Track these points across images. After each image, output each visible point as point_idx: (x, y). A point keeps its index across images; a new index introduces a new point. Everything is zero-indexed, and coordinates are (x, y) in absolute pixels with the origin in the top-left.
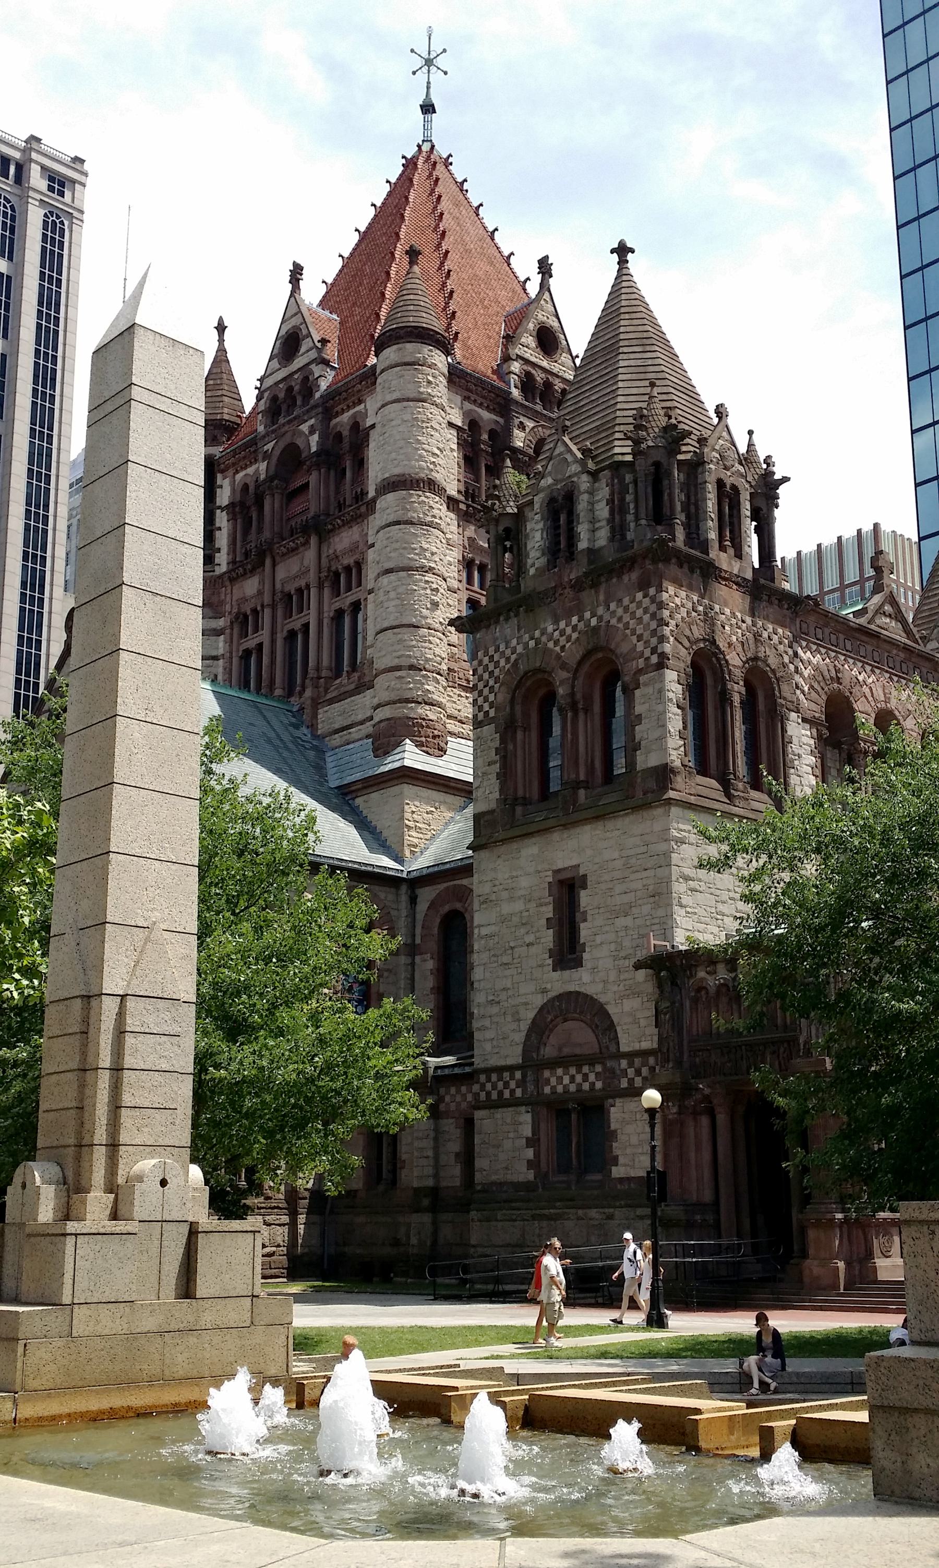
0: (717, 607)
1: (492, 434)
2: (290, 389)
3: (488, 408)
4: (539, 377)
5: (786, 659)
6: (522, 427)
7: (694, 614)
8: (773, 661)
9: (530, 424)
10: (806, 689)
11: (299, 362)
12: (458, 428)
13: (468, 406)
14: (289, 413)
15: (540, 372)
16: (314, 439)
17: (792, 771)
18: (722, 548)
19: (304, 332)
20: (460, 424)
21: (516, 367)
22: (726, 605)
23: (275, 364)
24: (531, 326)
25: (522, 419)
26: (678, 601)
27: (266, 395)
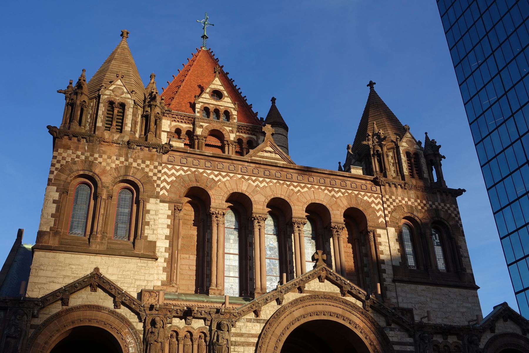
0: (96, 155)
4: (212, 108)
5: (151, 174)
6: (201, 126)
7: (76, 159)
8: (139, 176)
9: (205, 125)
10: (168, 187)
12: (168, 132)
13: (174, 124)
17: (146, 227)
18: (108, 129)
20: (169, 130)
22: (104, 153)
24: (208, 90)
25: (201, 124)
26: (65, 155)
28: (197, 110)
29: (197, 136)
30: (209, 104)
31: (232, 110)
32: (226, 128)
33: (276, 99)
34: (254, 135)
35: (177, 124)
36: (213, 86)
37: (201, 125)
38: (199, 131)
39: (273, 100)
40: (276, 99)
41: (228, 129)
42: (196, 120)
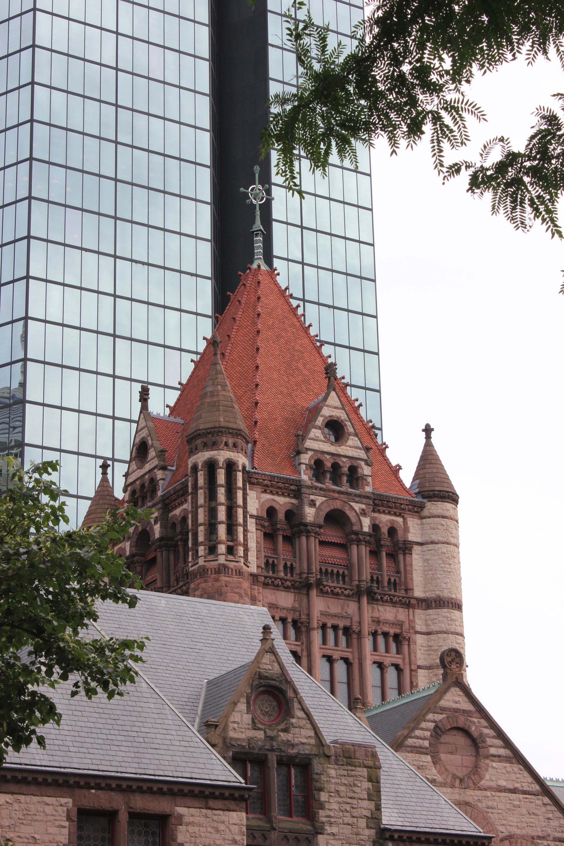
1: (289, 514)
2: (143, 486)
3: (283, 495)
6: (312, 504)
9: (319, 500)
11: (147, 467)
14: (152, 498)
15: (328, 457)
16: (157, 528)
19: (150, 442)
21: (305, 458)
23: (134, 466)
24: (320, 421)
25: (312, 497)
27: (129, 488)
28: (303, 467)
29: (306, 525)
30: (323, 452)
31: (362, 463)
32: (352, 504)
33: (433, 430)
34: (400, 515)
35: (269, 496)
36: (326, 412)
37: (312, 501)
38: (310, 514)
39: (428, 430)
40: (433, 430)
41: (357, 507)
42: (304, 490)
